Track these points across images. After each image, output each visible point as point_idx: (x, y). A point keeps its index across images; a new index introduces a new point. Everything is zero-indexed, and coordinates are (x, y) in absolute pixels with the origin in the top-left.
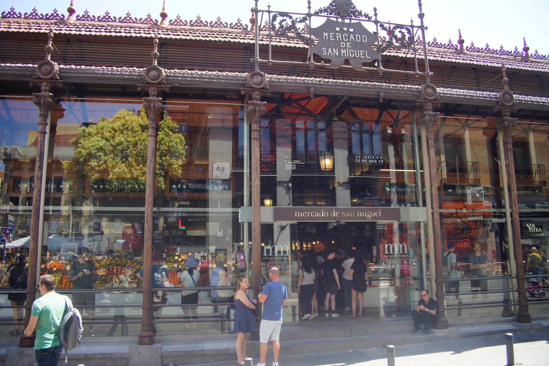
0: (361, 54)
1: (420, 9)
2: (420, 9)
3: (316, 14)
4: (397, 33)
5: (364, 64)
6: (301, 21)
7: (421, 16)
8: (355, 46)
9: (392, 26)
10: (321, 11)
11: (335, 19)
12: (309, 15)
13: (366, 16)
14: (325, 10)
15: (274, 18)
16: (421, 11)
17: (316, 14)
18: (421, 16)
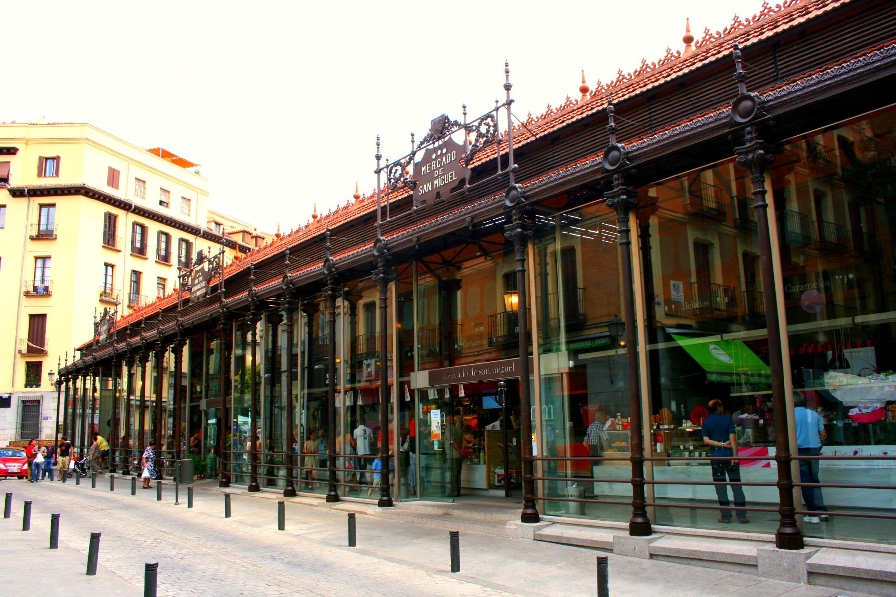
0: (448, 178)
1: (507, 76)
2: (507, 76)
3: (419, 148)
4: (483, 129)
5: (453, 190)
6: (408, 163)
7: (508, 87)
8: (446, 169)
9: (476, 124)
10: (422, 143)
11: (431, 147)
12: (414, 153)
13: (456, 123)
14: (425, 140)
15: (391, 172)
16: (507, 80)
17: (419, 148)
18: (508, 87)
